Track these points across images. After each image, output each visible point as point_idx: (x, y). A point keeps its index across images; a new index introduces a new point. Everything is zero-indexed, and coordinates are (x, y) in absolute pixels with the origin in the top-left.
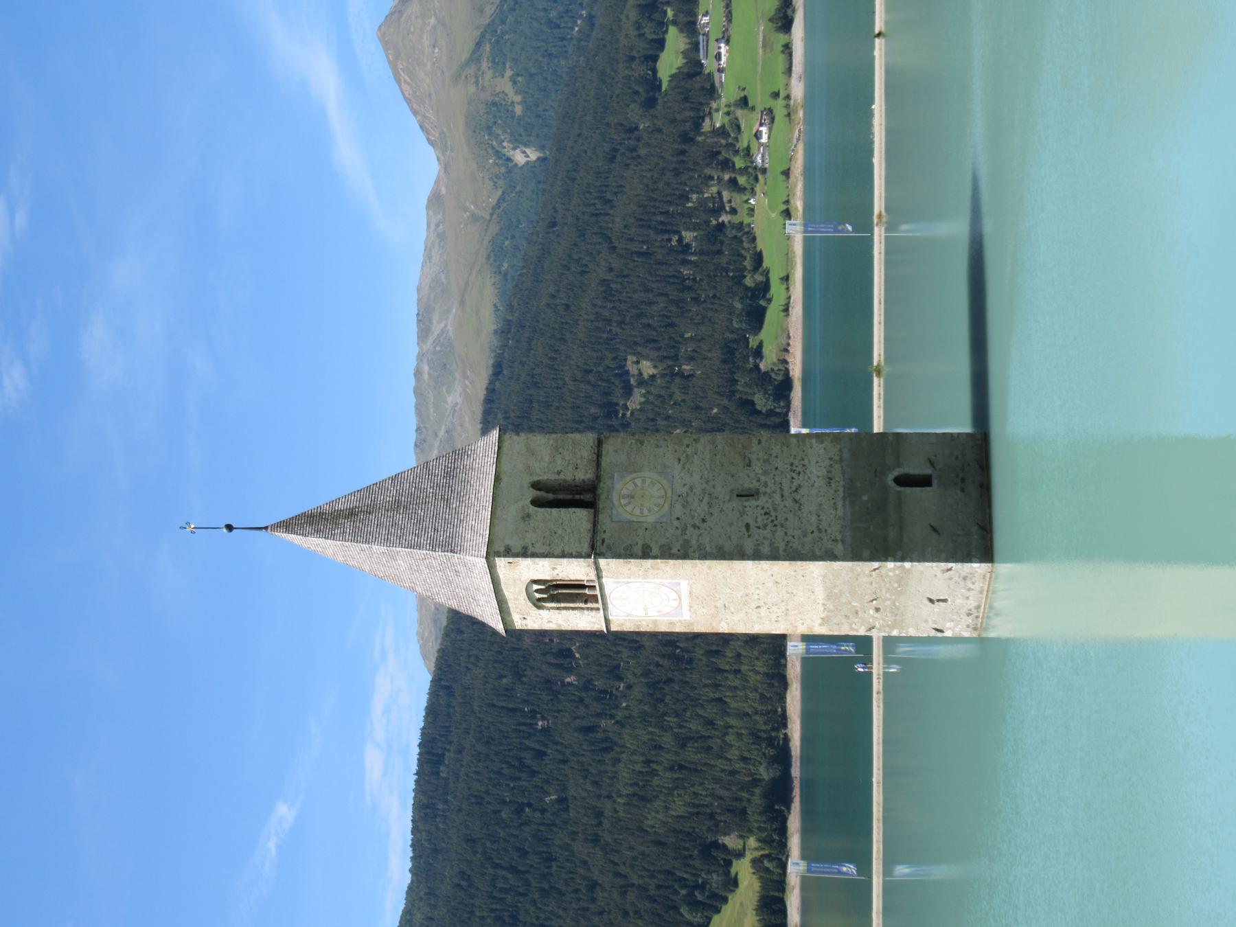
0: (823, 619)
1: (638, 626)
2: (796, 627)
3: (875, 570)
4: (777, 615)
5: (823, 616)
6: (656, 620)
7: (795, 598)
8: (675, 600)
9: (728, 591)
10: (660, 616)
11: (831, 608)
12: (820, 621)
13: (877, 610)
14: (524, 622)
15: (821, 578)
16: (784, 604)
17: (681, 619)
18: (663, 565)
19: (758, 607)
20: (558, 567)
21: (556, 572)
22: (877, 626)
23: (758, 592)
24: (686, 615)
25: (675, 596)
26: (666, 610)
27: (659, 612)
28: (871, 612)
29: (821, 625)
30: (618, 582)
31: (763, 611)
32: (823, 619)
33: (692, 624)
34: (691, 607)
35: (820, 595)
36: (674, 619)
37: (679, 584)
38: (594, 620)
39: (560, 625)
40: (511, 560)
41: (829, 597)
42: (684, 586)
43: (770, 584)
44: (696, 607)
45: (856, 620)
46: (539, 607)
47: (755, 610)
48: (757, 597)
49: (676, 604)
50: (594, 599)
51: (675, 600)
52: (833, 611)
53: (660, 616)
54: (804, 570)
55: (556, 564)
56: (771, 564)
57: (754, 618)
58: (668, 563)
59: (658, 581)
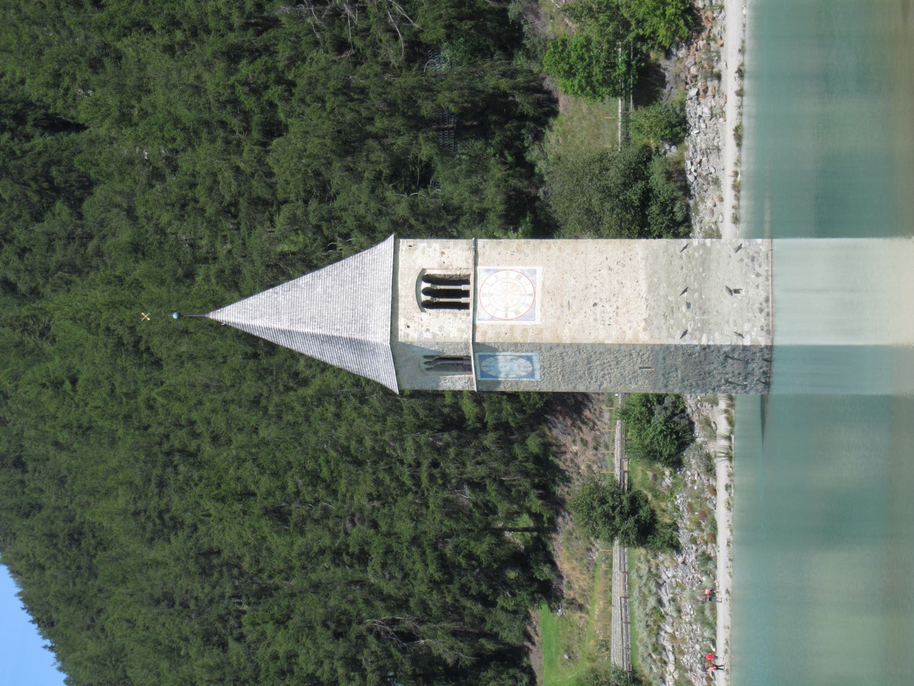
0: (645, 320)
1: (498, 334)
2: (624, 332)
3: (685, 248)
4: (611, 315)
5: (646, 316)
6: (512, 328)
7: (624, 290)
8: (530, 295)
9: (573, 282)
10: (517, 319)
11: (652, 304)
12: (643, 324)
13: (688, 305)
14: (407, 331)
15: (643, 263)
16: (615, 299)
17: (533, 323)
18: (525, 246)
19: (595, 304)
20: (446, 251)
21: (444, 258)
22: (690, 330)
23: (596, 283)
24: (538, 321)
25: (530, 289)
26: (523, 310)
27: (516, 312)
28: (684, 308)
29: (645, 329)
30: (488, 270)
31: (599, 308)
32: (645, 320)
33: (541, 331)
34: (542, 306)
35: (643, 287)
36: (528, 323)
37: (535, 272)
38: (464, 326)
39: (434, 335)
40: (411, 242)
41: (649, 291)
42: (539, 269)
43: (605, 272)
44: (546, 305)
45: (672, 322)
46: (423, 311)
47: (593, 308)
48: (594, 290)
49: (529, 300)
50: (465, 306)
51: (530, 295)
52: (654, 308)
53: (517, 319)
54: (630, 250)
55: (445, 247)
56: (607, 244)
57: (591, 320)
58: (528, 243)
59: (519, 268)
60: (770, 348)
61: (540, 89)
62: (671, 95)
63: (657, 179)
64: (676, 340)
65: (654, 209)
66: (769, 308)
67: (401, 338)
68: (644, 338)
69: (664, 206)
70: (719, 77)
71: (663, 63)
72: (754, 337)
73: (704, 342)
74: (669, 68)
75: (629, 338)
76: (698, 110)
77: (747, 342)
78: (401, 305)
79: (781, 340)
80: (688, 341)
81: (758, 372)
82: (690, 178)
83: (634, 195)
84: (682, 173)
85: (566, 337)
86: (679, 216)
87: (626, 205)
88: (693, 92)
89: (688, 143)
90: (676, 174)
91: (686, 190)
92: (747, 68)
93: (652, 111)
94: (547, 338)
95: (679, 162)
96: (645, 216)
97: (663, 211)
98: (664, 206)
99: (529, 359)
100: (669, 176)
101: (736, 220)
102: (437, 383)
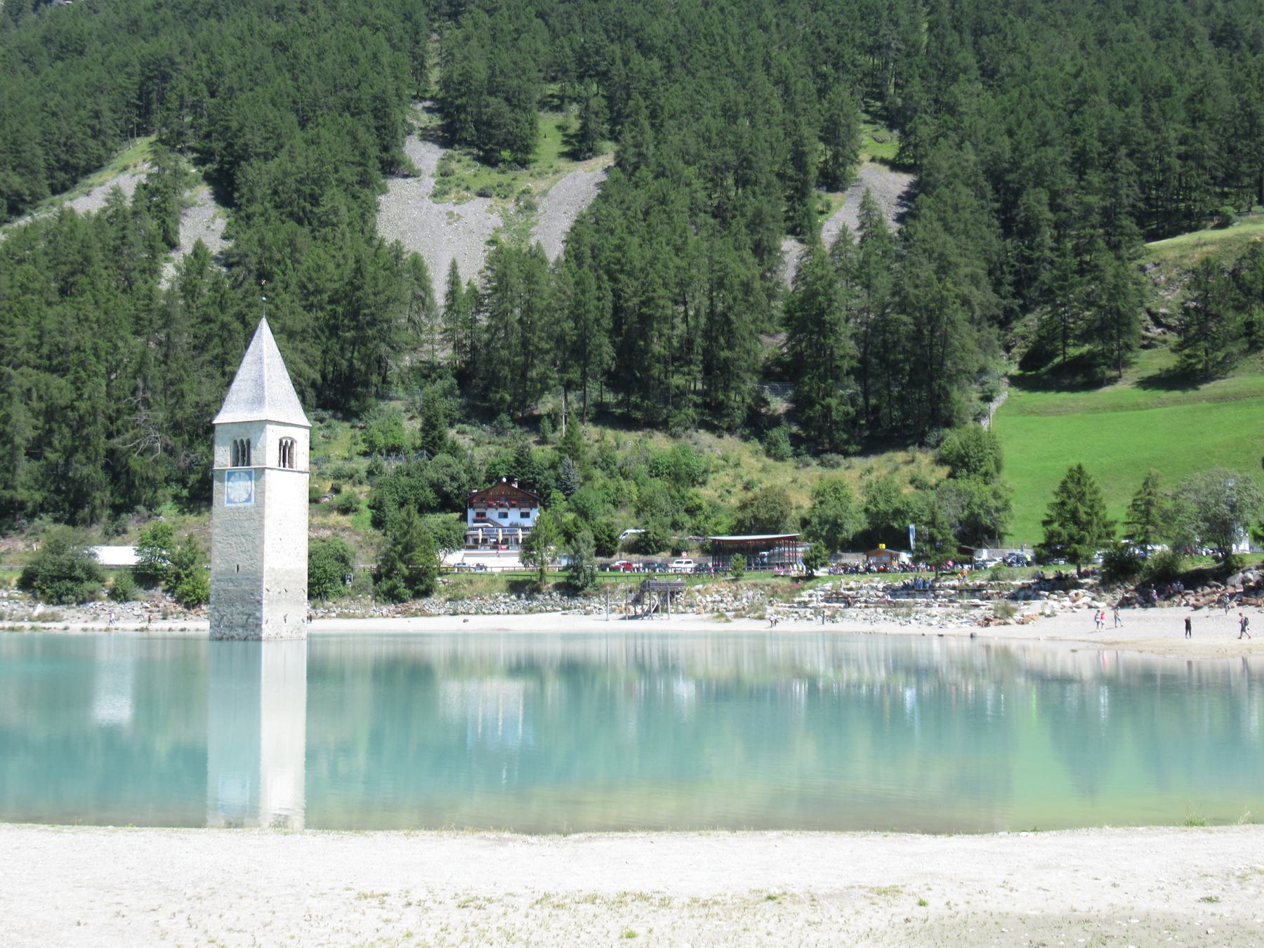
60: (259, 639)
61: (92, 522)
62: (140, 592)
63: (89, 586)
64: (265, 586)
65: (69, 584)
66: (278, 638)
67: (269, 427)
68: (266, 567)
69: (72, 590)
70: (164, 619)
71: (160, 589)
72: (266, 630)
73: (264, 602)
74: (158, 591)
75: (266, 558)
76: (137, 607)
77: (264, 626)
78: (282, 428)
79: (264, 645)
80: (265, 592)
81: (234, 633)
82: (91, 604)
83: (78, 573)
84: (93, 600)
85: (267, 522)
86: (64, 598)
87: (72, 567)
88: (146, 604)
89: (113, 603)
90: (93, 596)
91: (83, 602)
92: (187, 633)
93: (131, 582)
94: (267, 511)
95: (100, 599)
96: (65, 578)
97: (67, 589)
98: (72, 590)
99: (248, 500)
100: (92, 592)
101: (85, 630)
102: (223, 445)
